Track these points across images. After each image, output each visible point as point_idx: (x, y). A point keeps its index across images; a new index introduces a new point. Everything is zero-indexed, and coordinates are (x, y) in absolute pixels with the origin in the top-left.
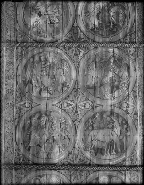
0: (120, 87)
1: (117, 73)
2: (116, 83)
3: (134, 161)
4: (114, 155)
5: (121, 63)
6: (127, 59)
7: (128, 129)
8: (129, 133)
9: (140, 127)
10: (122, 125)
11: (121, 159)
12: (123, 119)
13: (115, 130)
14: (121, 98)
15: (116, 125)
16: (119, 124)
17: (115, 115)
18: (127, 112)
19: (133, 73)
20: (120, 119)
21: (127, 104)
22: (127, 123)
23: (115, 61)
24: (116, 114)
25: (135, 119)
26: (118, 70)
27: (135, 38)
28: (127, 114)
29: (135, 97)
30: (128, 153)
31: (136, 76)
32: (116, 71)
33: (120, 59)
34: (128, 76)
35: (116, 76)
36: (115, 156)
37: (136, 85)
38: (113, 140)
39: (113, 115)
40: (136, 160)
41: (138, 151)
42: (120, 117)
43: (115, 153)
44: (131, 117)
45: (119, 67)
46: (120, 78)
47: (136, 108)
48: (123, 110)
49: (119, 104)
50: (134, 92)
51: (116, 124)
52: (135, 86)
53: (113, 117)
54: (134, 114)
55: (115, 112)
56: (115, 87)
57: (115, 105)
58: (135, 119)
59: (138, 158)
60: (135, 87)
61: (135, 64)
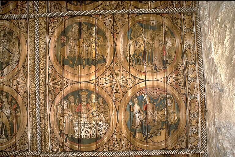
0: (10, 63)
1: (7, 47)
2: (6, 59)
3: (25, 145)
4: (3, 138)
5: (12, 36)
6: (19, 32)
7: (18, 110)
8: (18, 114)
9: (30, 106)
10: (11, 105)
11: (11, 143)
12: (13, 98)
13: (4, 110)
14: (11, 75)
15: (5, 106)
16: (9, 104)
17: (4, 94)
18: (16, 90)
19: (24, 47)
20: (10, 98)
21: (17, 81)
22: (16, 102)
23: (5, 35)
24: (6, 92)
25: (25, 98)
26: (8, 44)
27: (27, 9)
28: (16, 93)
29: (25, 73)
30: (19, 135)
31: (27, 50)
32: (6, 46)
33: (11, 33)
34: (18, 50)
35: (6, 51)
36: (5, 140)
37: (26, 60)
38: (2, 122)
39: (2, 94)
40: (27, 144)
41: (29, 134)
42: (9, 96)
43: (5, 137)
44: (20, 95)
45: (10, 41)
46: (10, 53)
47: (26, 85)
48: (13, 88)
49: (9, 81)
50: (24, 67)
51: (6, 105)
52: (25, 61)
53: (2, 96)
54: (24, 93)
55: (4, 90)
56: (4, 63)
57: (4, 83)
58: (25, 98)
59: (29, 142)
60: (25, 63)
61: (26, 37)
